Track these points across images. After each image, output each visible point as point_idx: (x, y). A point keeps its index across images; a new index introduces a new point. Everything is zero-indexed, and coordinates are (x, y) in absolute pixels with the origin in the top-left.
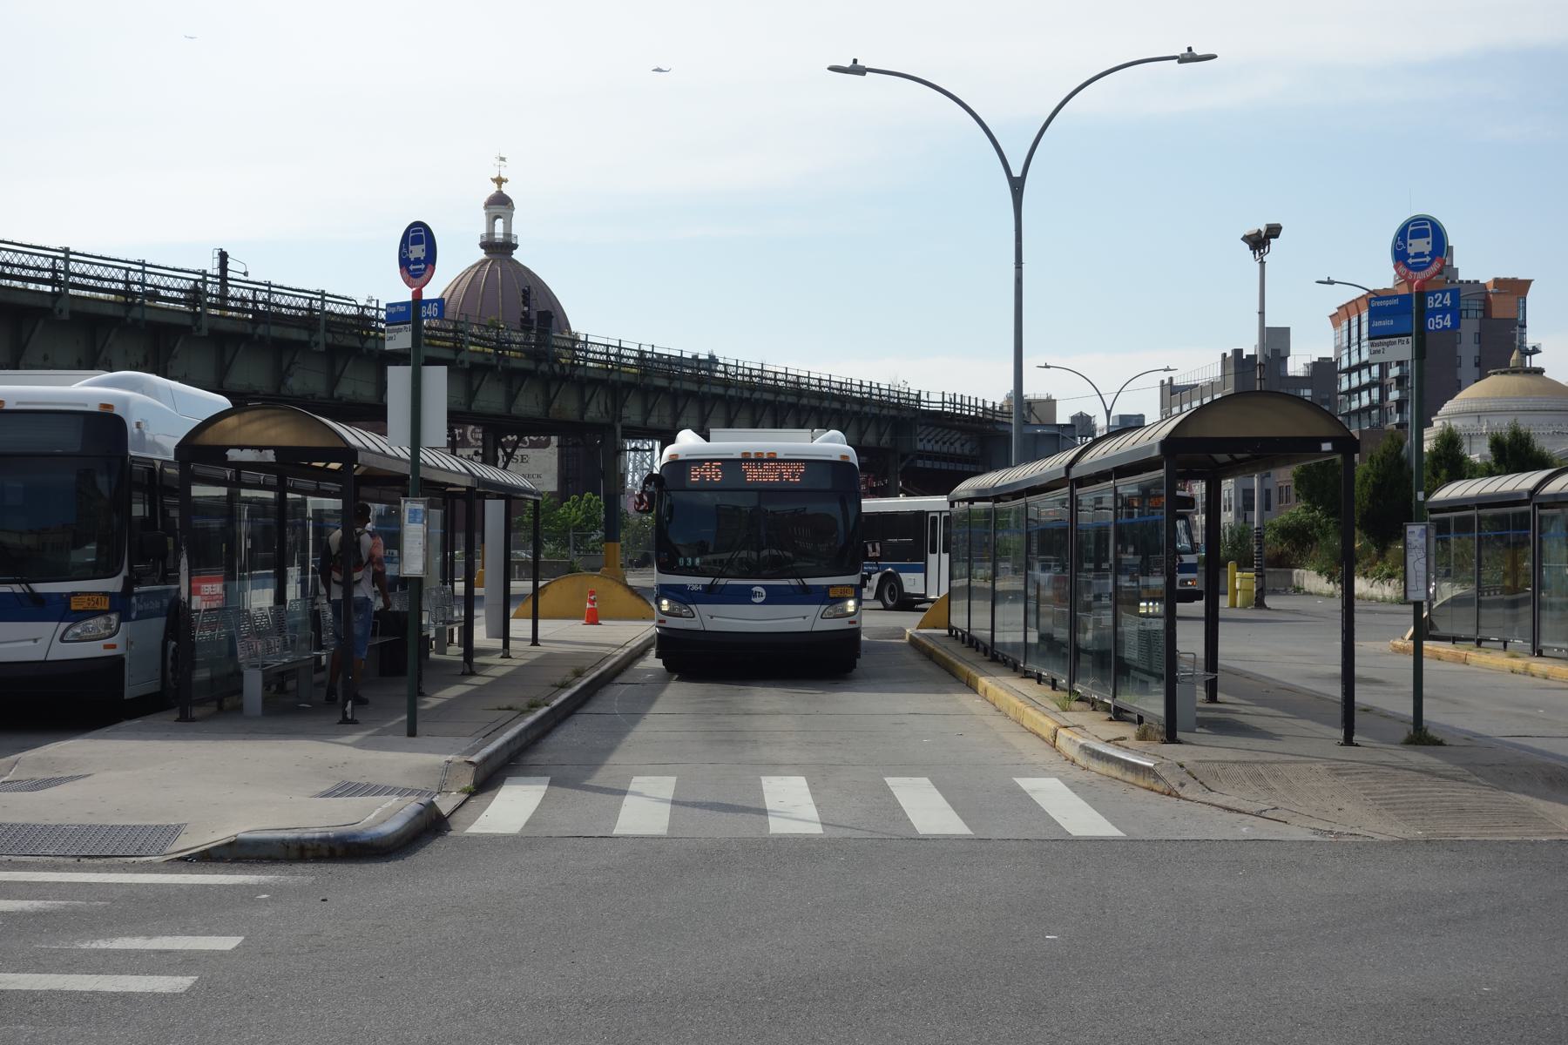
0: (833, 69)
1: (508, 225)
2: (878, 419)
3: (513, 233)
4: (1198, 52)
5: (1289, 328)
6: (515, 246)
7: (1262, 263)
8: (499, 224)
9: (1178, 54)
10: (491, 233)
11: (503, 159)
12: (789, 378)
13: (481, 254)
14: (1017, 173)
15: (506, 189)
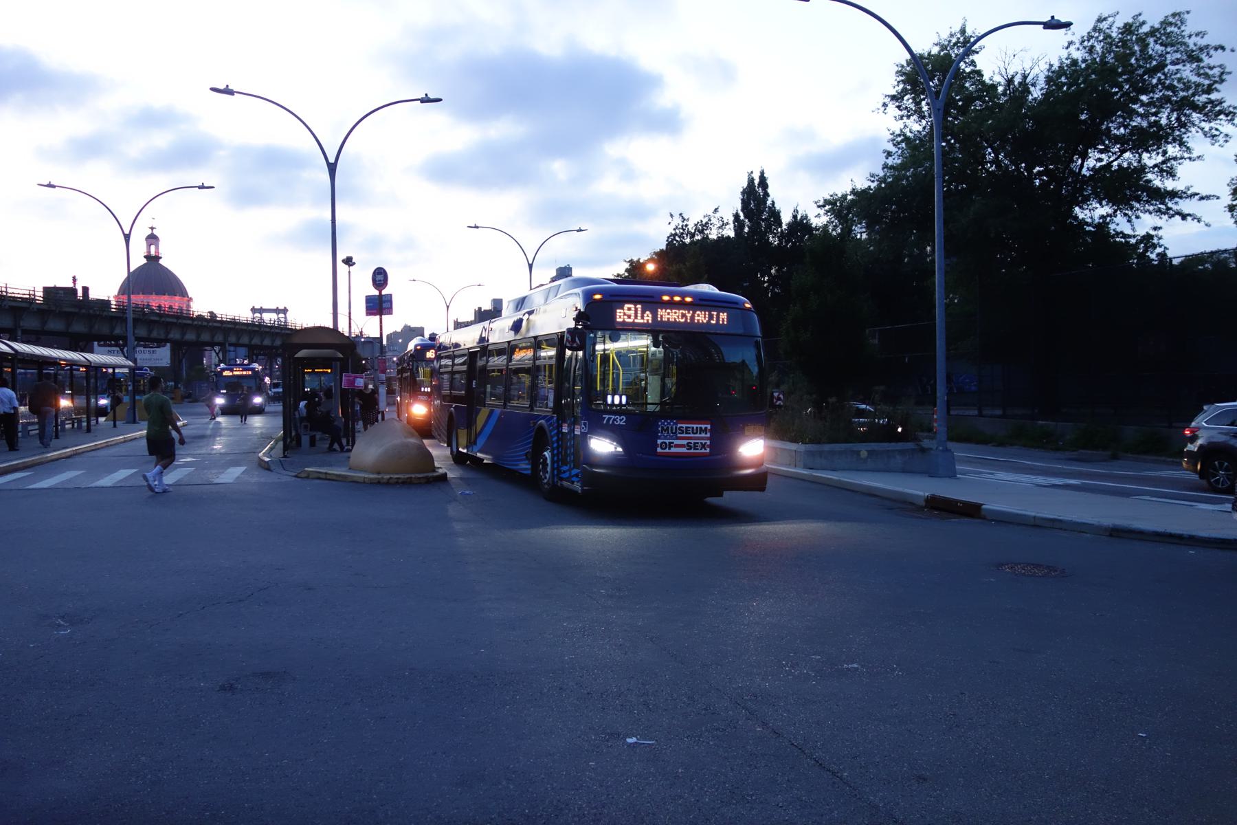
0: (39, 185)
1: (157, 248)
2: (277, 334)
3: (161, 250)
4: (206, 185)
5: (502, 300)
6: (161, 258)
7: (349, 272)
8: (153, 248)
9: (198, 185)
10: (149, 252)
11: (153, 219)
12: (228, 317)
13: (145, 261)
14: (127, 232)
15: (155, 232)
